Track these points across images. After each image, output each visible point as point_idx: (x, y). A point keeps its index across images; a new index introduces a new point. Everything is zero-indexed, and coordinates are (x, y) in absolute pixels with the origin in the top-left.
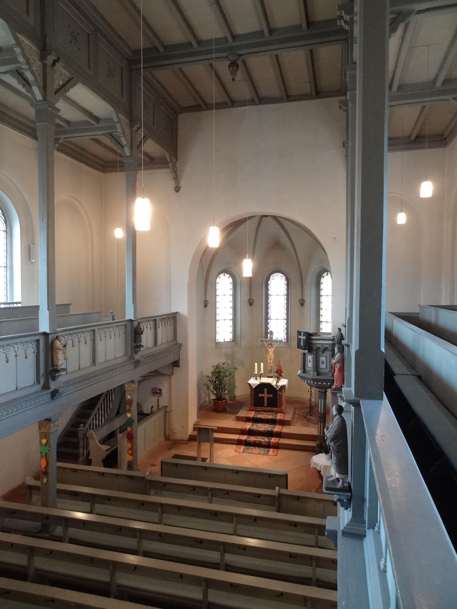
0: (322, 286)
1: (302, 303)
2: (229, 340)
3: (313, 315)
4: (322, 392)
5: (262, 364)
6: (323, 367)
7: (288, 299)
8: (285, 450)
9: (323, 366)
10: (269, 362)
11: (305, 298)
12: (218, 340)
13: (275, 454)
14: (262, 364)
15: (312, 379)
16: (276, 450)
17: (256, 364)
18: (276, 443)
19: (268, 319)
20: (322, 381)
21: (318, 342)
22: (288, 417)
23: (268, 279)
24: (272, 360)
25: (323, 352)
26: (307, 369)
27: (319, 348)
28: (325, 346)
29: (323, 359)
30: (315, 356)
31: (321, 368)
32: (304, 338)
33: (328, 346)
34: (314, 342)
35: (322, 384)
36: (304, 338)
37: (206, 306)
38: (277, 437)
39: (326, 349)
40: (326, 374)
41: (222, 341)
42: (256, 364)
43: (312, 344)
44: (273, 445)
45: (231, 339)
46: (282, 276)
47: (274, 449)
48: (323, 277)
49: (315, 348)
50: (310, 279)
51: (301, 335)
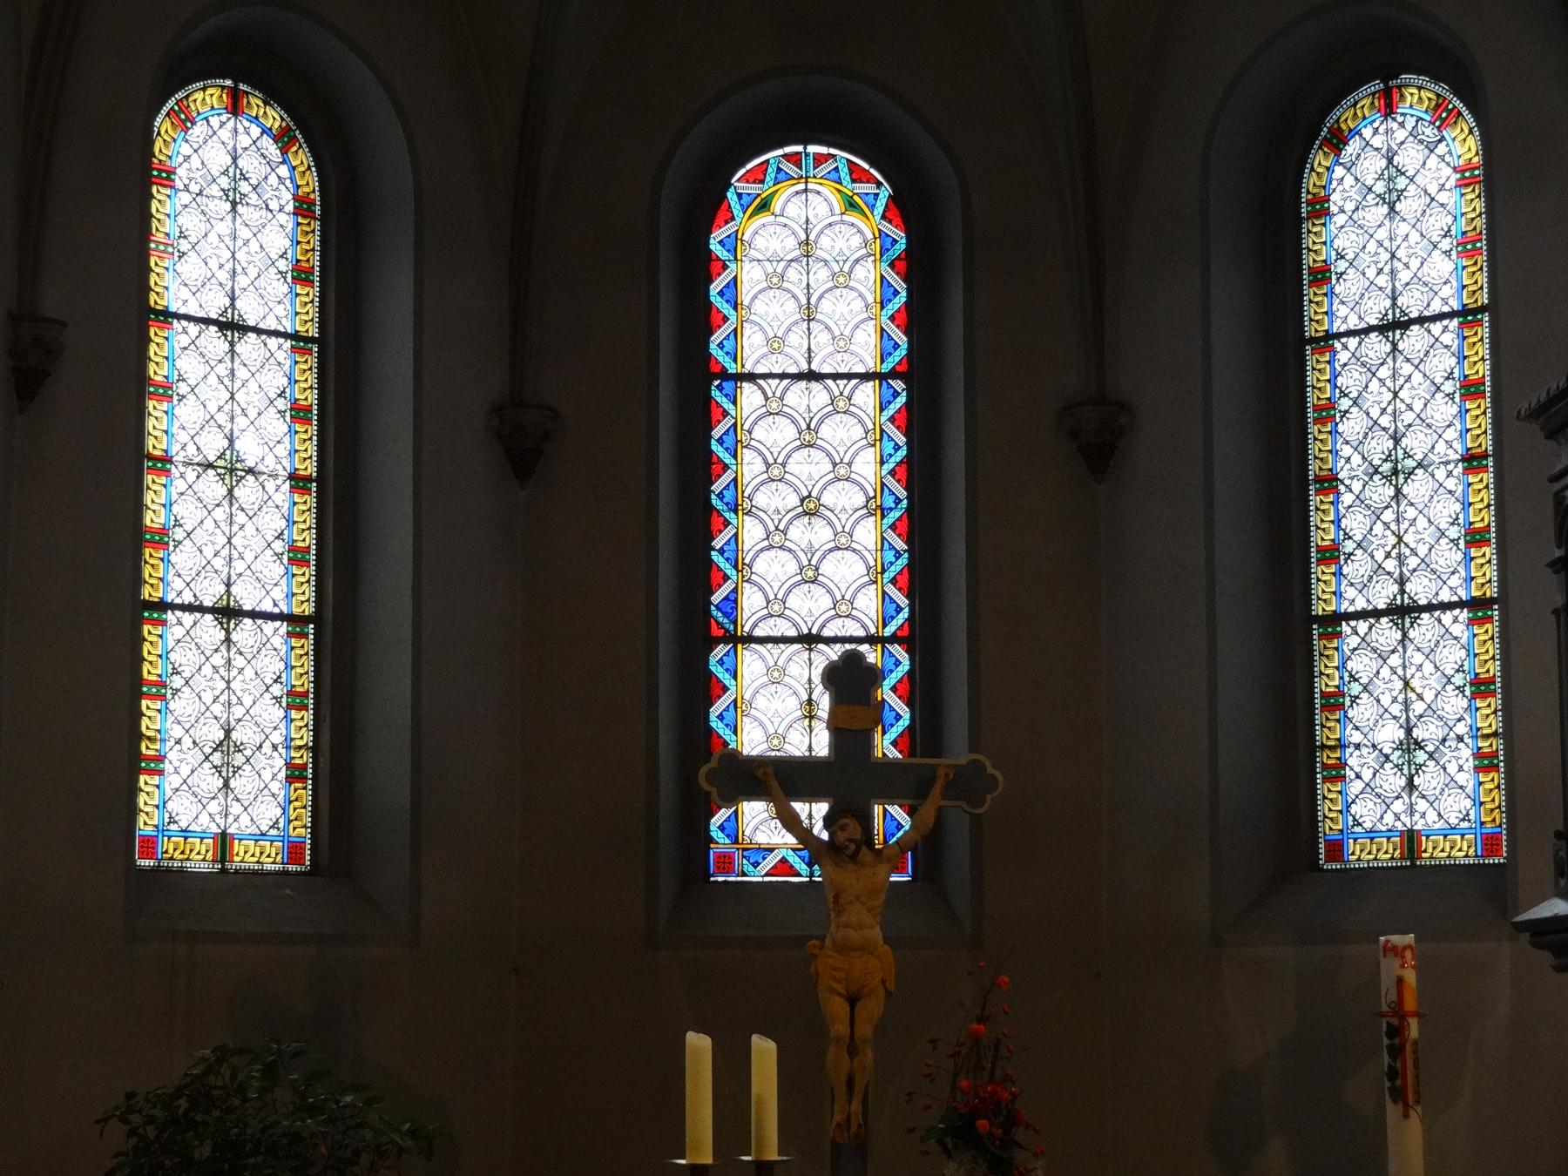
1: (1098, 439)
2: (271, 858)
5: (764, 1050)
7: (921, 423)
10: (842, 1028)
12: (149, 845)
14: (764, 1050)
17: (699, 1044)
19: (712, 643)
23: (706, 205)
24: (872, 1008)
37: (29, 383)
41: (200, 860)
42: (699, 1044)
45: (294, 851)
46: (857, 175)
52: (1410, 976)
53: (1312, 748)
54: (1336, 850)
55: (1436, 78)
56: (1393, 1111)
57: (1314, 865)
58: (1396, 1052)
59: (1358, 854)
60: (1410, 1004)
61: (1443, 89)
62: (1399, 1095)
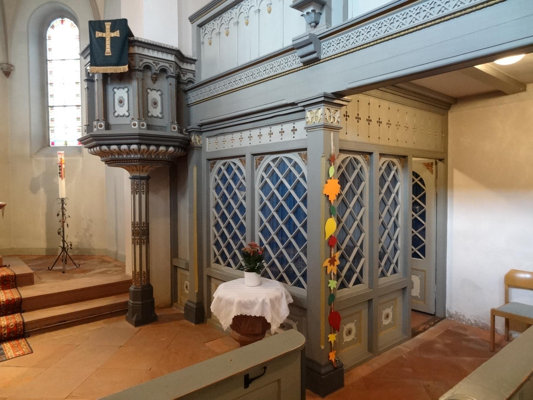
0: (49, 44)
3: (35, 92)
4: (141, 178)
6: (155, 115)
8: (47, 335)
9: (156, 112)
11: (12, 62)
13: (25, 349)
15: (141, 137)
16: (22, 342)
18: (16, 325)
20: (158, 140)
21: (146, 52)
22: (20, 269)
25: (155, 80)
26: (112, 120)
27: (148, 67)
28: (162, 64)
29: (154, 95)
30: (140, 85)
31: (152, 116)
32: (117, 34)
33: (167, 65)
34: (137, 50)
35: (158, 150)
36: (117, 34)
38: (13, 313)
39: (163, 71)
40: (162, 128)
43: (132, 56)
44: (9, 333)
47: (14, 343)
48: (53, 27)
49: (139, 64)
50: (23, 26)
51: (103, 30)
52: (63, 158)
53: (49, 127)
54: (53, 144)
55: (71, 20)
56: (60, 179)
57: (49, 146)
58: (60, 170)
59: (57, 144)
60: (63, 162)
61: (72, 22)
62: (61, 176)
